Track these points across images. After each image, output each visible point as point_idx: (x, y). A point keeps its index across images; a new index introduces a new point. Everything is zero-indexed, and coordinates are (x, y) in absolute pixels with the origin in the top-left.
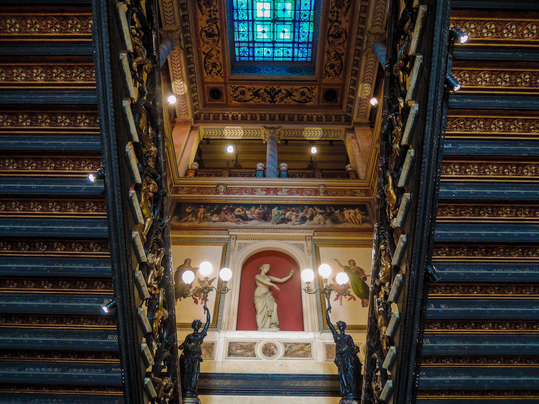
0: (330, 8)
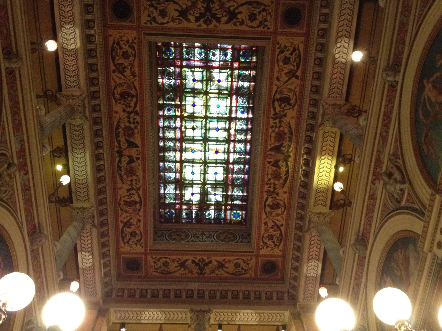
0: (139, 127)
